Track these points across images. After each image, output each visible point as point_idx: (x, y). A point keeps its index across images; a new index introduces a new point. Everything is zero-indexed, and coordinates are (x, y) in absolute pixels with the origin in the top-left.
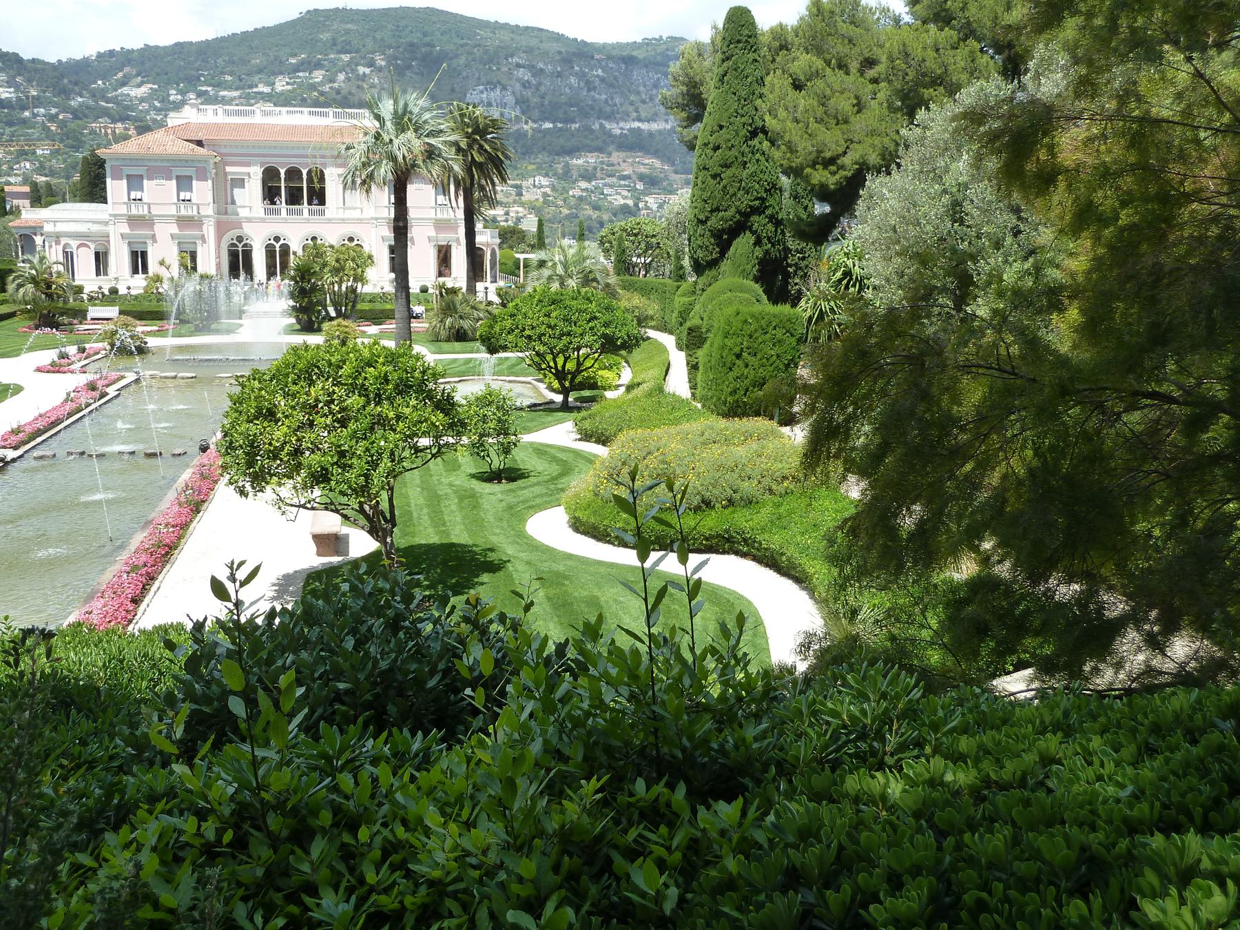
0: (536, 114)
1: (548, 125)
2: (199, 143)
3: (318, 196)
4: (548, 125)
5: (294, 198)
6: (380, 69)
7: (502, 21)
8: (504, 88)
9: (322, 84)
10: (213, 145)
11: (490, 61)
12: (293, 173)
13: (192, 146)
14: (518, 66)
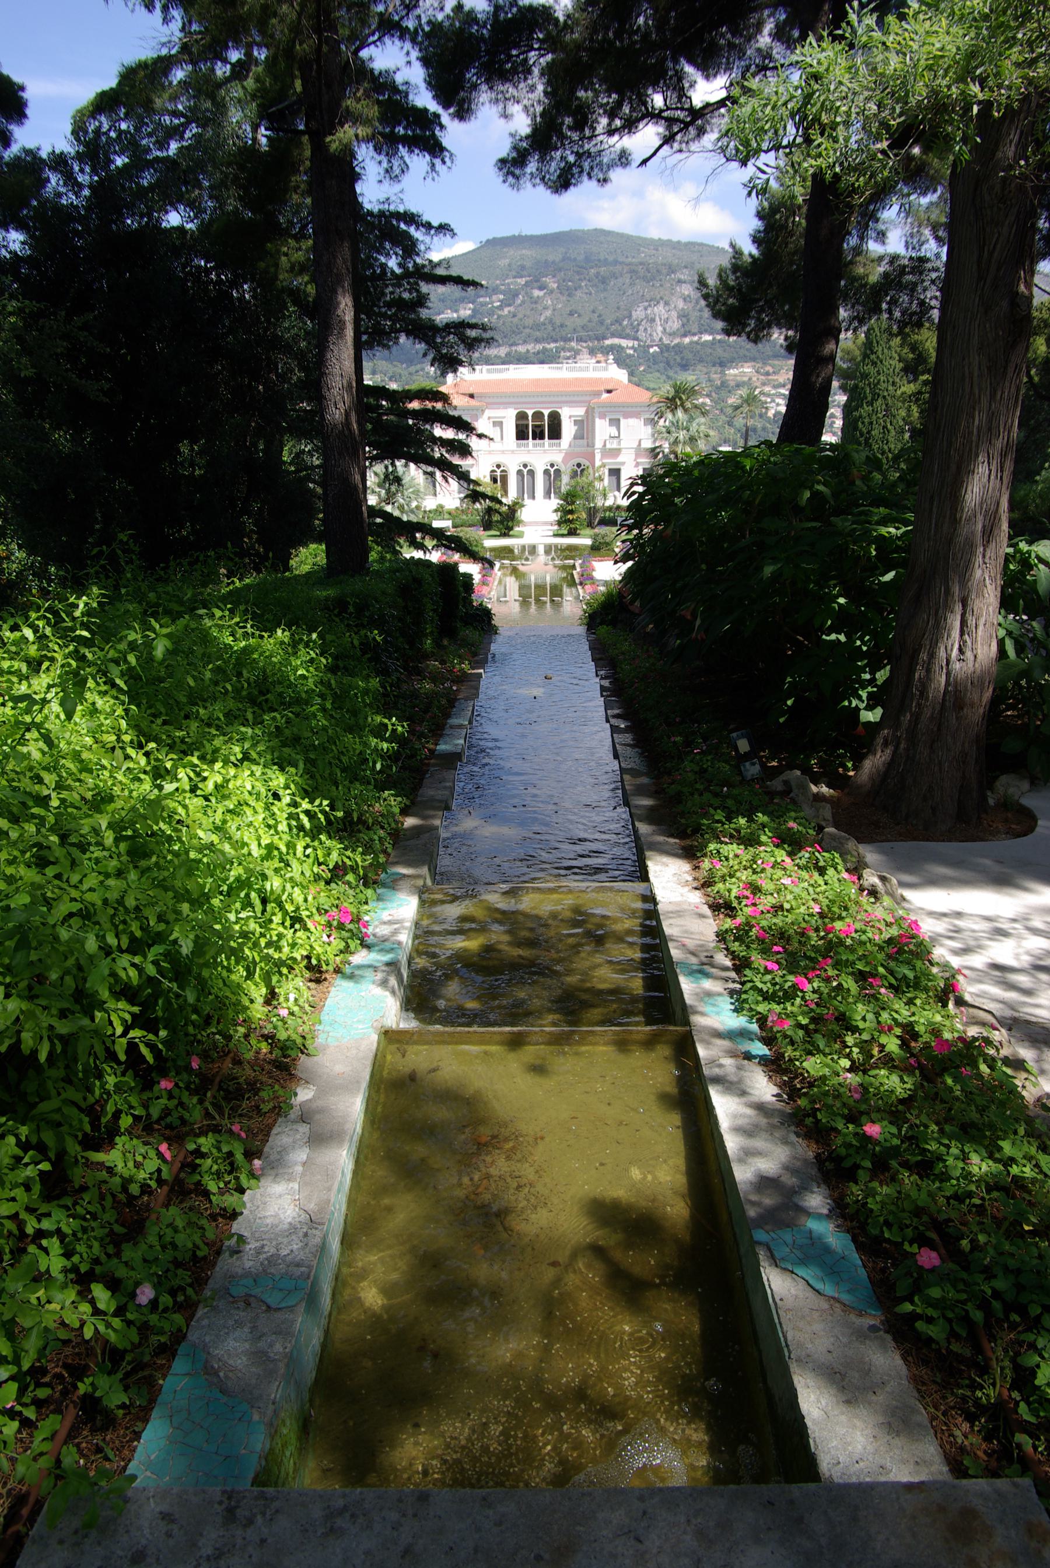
0: (695, 328)
1: (708, 338)
2: (472, 396)
3: (555, 433)
4: (708, 338)
5: (538, 435)
6: (552, 292)
7: (665, 237)
8: (667, 304)
9: (500, 308)
10: (482, 396)
11: (653, 279)
12: (538, 415)
13: (467, 399)
14: (680, 281)
